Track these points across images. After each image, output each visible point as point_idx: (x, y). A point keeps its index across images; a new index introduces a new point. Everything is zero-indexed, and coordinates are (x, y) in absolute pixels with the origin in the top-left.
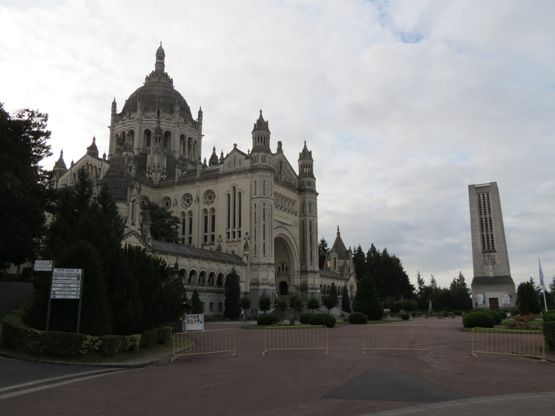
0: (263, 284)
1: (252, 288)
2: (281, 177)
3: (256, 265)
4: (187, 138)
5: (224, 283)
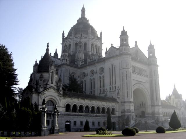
0: (127, 112)
1: (122, 114)
2: (138, 59)
3: (123, 102)
4: (95, 45)
5: (106, 112)
